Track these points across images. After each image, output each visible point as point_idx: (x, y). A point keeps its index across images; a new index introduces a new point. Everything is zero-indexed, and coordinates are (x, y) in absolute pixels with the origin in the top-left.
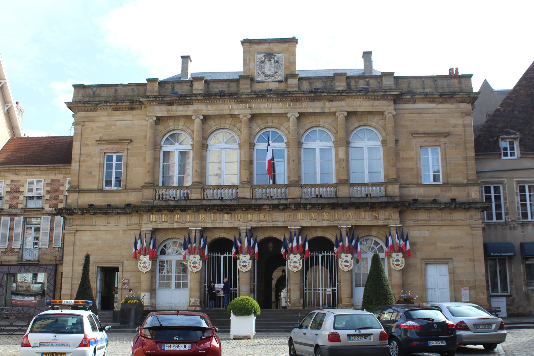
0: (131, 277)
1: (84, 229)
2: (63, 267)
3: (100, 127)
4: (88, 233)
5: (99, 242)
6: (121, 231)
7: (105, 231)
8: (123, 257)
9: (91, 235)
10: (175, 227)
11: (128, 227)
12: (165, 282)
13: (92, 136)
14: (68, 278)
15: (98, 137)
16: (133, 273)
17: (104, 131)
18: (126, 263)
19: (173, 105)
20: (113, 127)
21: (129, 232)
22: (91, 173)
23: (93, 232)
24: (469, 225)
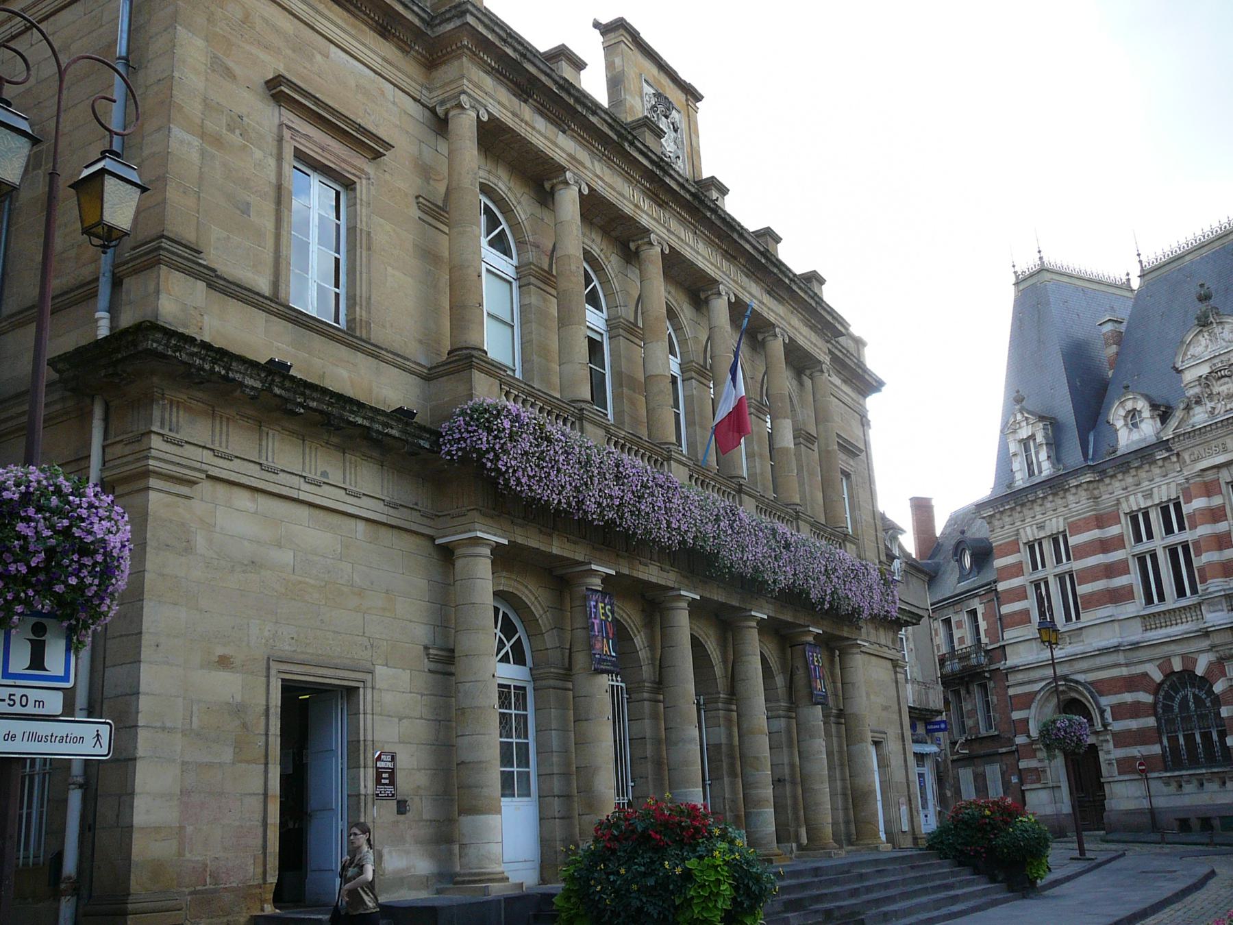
0: (400, 742)
1: (234, 477)
2: (142, 665)
3: (277, 30)
4: (243, 500)
5: (286, 557)
6: (361, 526)
7: (304, 512)
8: (372, 646)
9: (256, 513)
10: (554, 552)
11: (391, 511)
12: (515, 769)
13: (248, 47)
14: (163, 729)
15: (272, 66)
16: (405, 722)
17: (289, 52)
18: (380, 670)
19: (525, 101)
20: (319, 58)
21: (386, 535)
22: (245, 209)
23: (265, 503)
24: (891, 660)
